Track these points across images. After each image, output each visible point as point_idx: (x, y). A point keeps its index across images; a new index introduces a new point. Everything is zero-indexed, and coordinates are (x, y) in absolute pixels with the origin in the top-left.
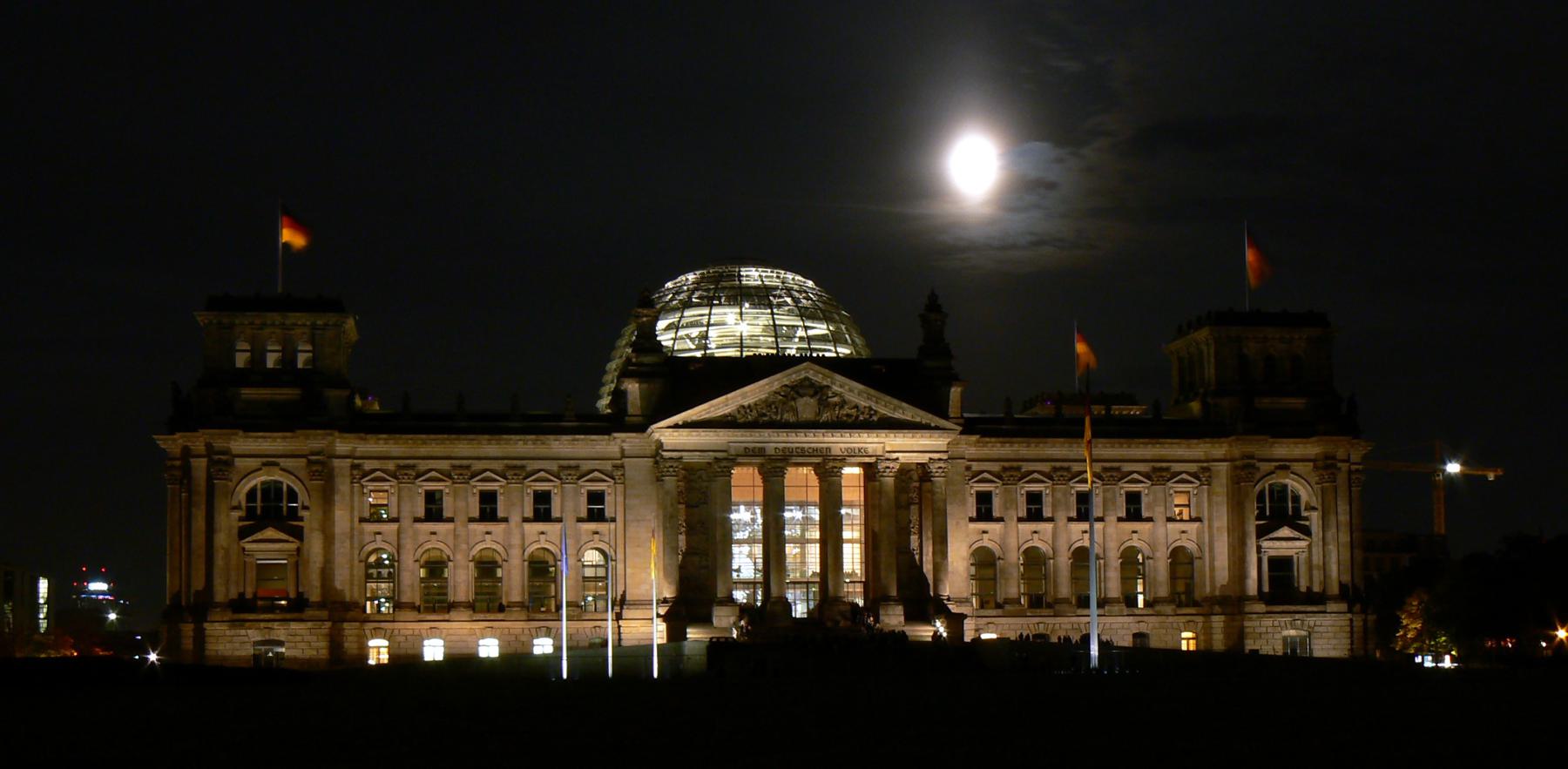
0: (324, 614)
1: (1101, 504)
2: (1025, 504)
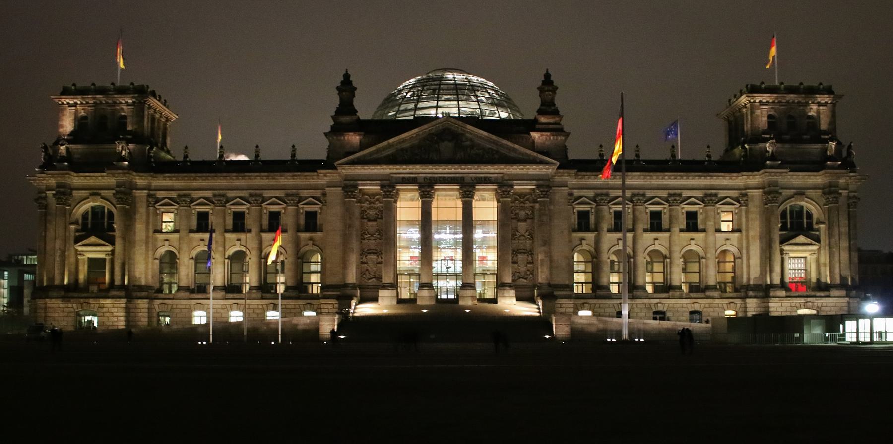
0: (123, 294)
1: (668, 220)
2: (613, 219)
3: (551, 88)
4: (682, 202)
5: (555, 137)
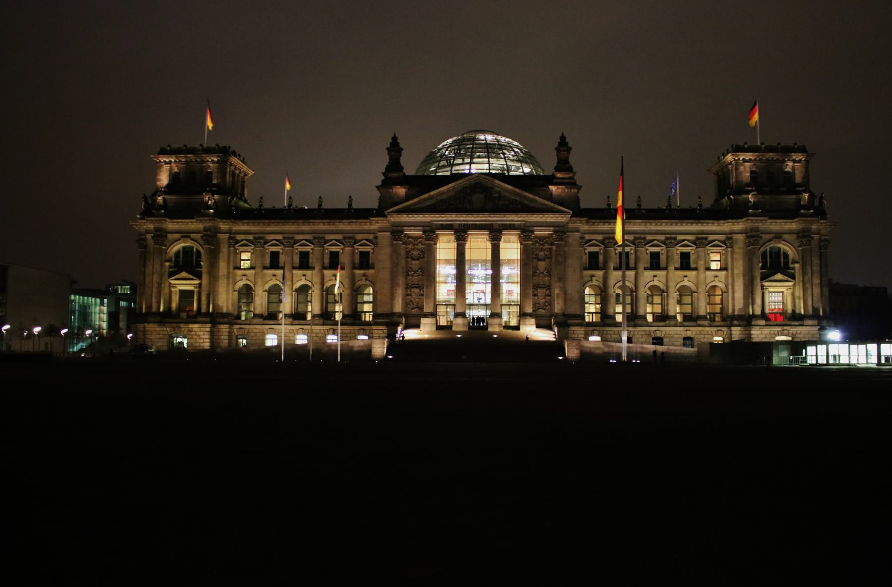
0: (208, 319)
1: (665, 260)
3: (566, 149)
4: (676, 245)
5: (569, 190)
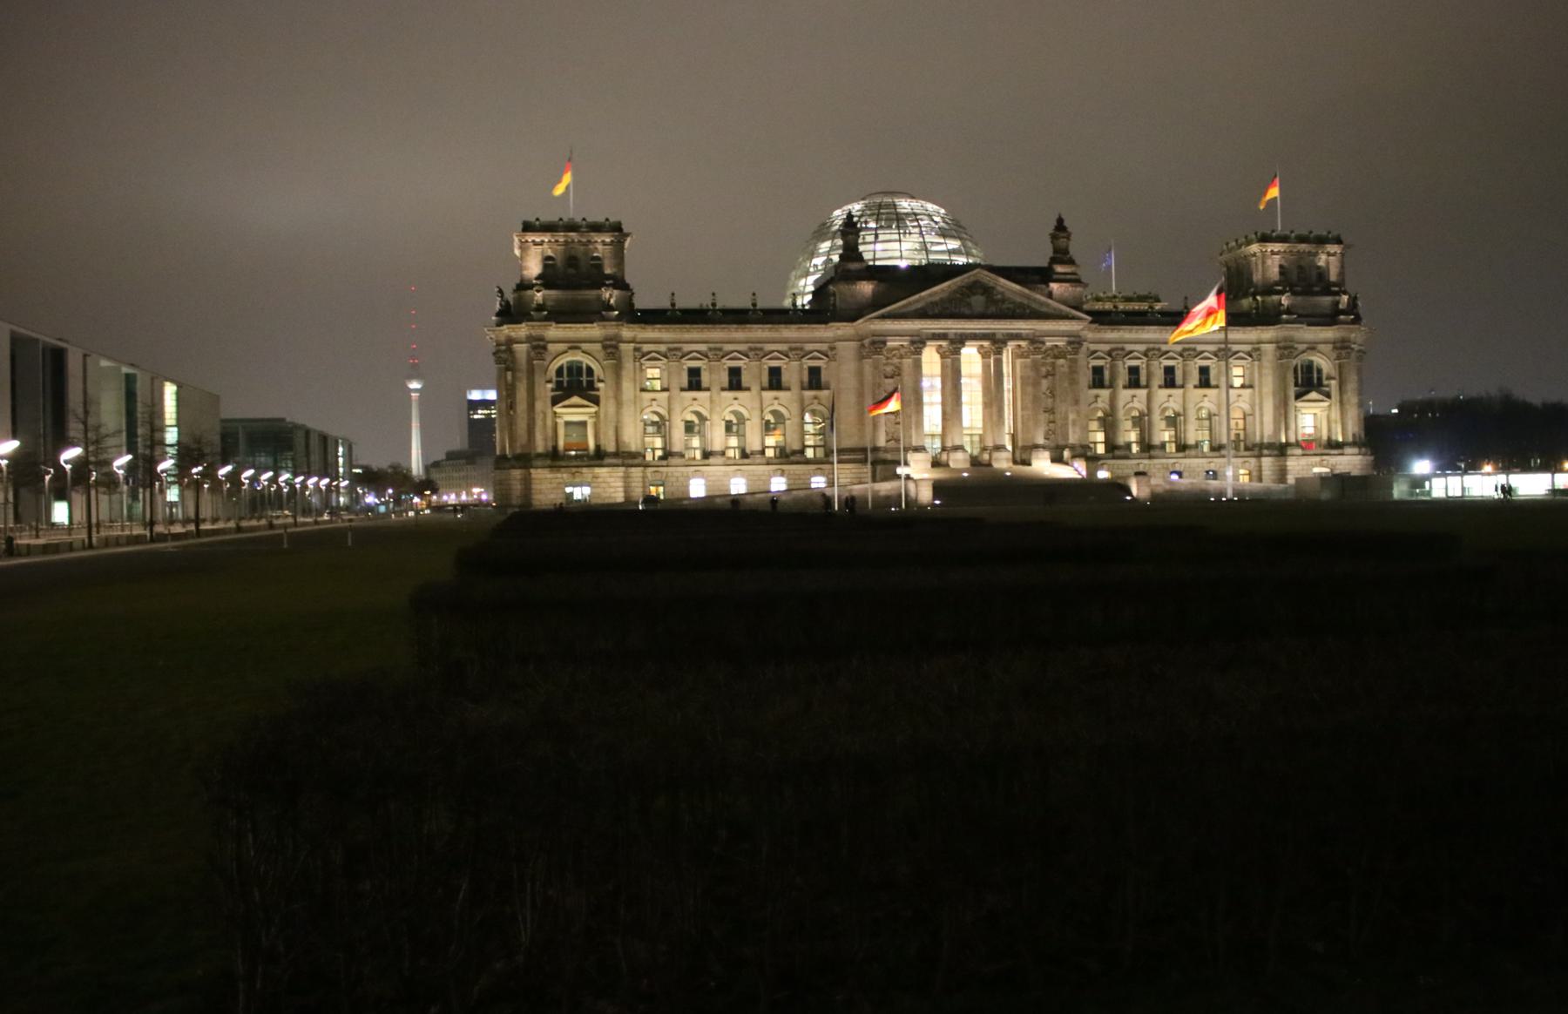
3: (1065, 235)
